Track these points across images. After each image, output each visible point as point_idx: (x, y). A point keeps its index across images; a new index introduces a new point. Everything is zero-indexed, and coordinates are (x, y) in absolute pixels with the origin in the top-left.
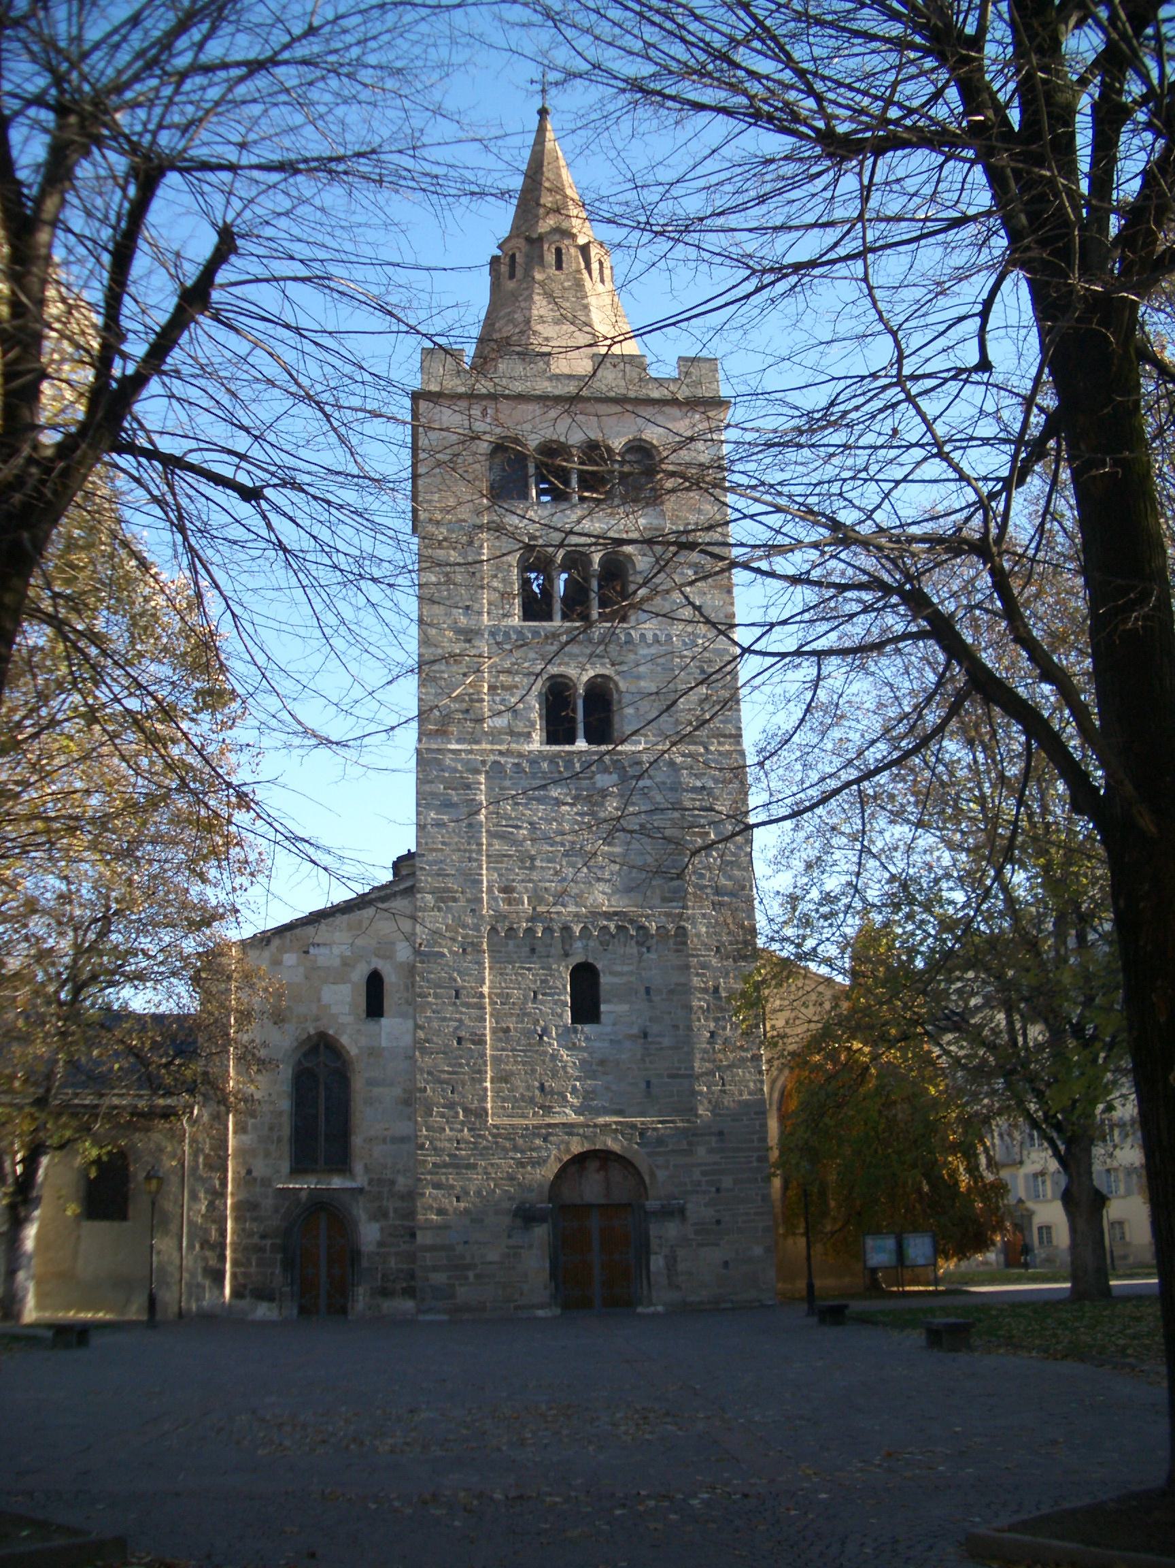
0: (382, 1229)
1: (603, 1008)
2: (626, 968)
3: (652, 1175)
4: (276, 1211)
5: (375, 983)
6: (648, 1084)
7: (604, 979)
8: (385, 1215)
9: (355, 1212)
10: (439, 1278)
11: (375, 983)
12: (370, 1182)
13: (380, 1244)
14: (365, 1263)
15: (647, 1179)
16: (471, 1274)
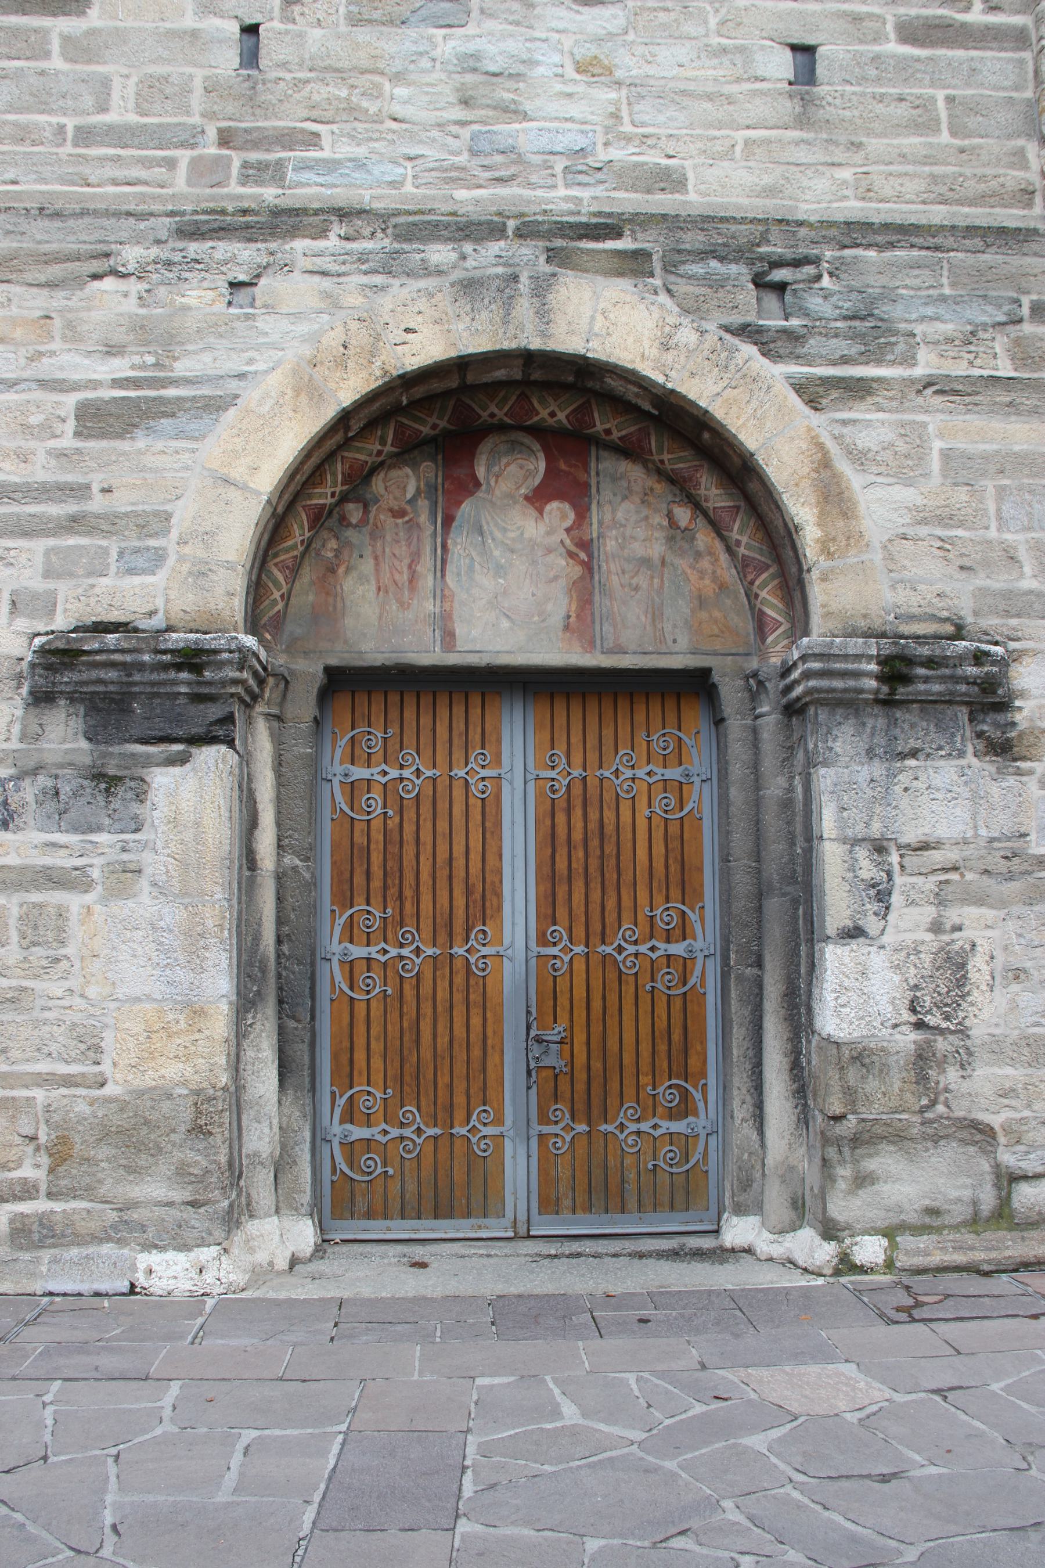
6: (804, 51)
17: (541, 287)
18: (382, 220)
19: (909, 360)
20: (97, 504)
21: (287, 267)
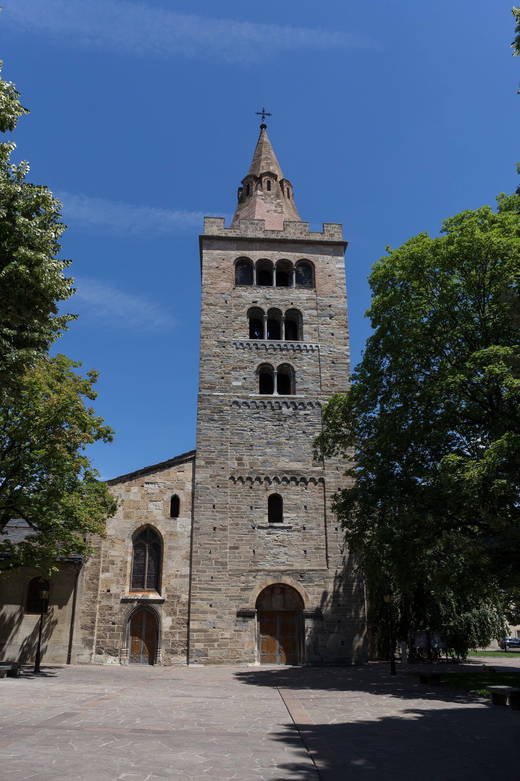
0: (173, 620)
1: (284, 515)
2: (295, 497)
3: (307, 597)
4: (121, 611)
5: (175, 501)
6: (305, 551)
7: (285, 502)
8: (175, 614)
9: (160, 612)
10: (199, 646)
11: (175, 501)
12: (168, 596)
13: (172, 628)
14: (163, 637)
15: (304, 598)
16: (216, 644)
17: (281, 577)
18: (267, 570)
19: (314, 583)
20: (243, 597)
21: (258, 575)
